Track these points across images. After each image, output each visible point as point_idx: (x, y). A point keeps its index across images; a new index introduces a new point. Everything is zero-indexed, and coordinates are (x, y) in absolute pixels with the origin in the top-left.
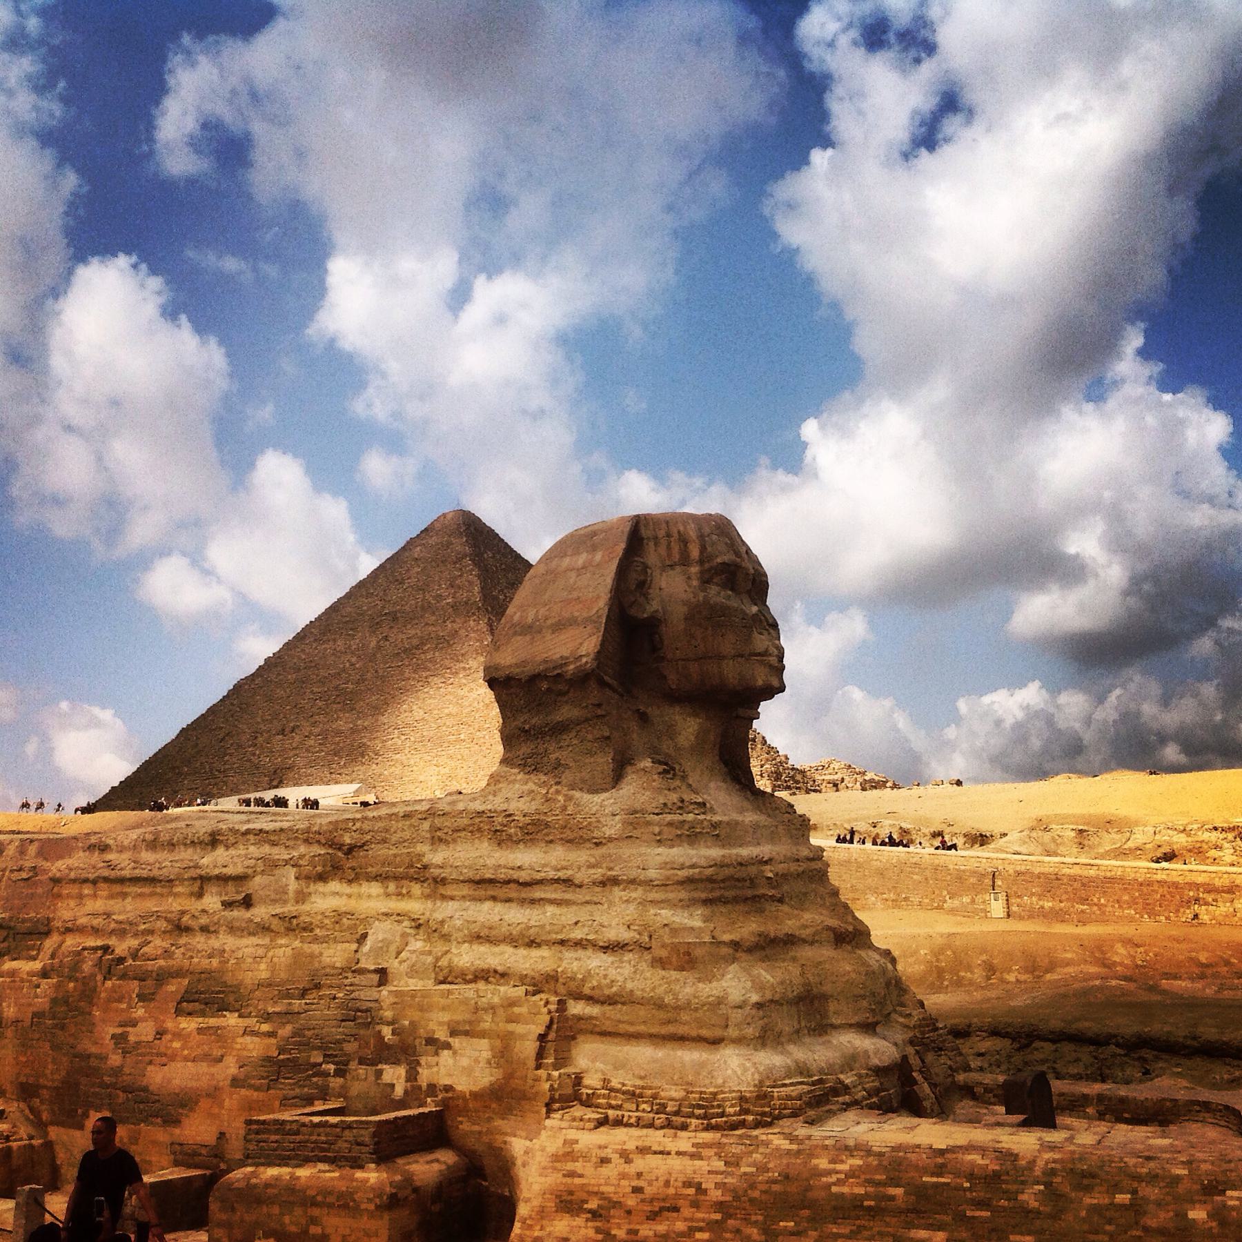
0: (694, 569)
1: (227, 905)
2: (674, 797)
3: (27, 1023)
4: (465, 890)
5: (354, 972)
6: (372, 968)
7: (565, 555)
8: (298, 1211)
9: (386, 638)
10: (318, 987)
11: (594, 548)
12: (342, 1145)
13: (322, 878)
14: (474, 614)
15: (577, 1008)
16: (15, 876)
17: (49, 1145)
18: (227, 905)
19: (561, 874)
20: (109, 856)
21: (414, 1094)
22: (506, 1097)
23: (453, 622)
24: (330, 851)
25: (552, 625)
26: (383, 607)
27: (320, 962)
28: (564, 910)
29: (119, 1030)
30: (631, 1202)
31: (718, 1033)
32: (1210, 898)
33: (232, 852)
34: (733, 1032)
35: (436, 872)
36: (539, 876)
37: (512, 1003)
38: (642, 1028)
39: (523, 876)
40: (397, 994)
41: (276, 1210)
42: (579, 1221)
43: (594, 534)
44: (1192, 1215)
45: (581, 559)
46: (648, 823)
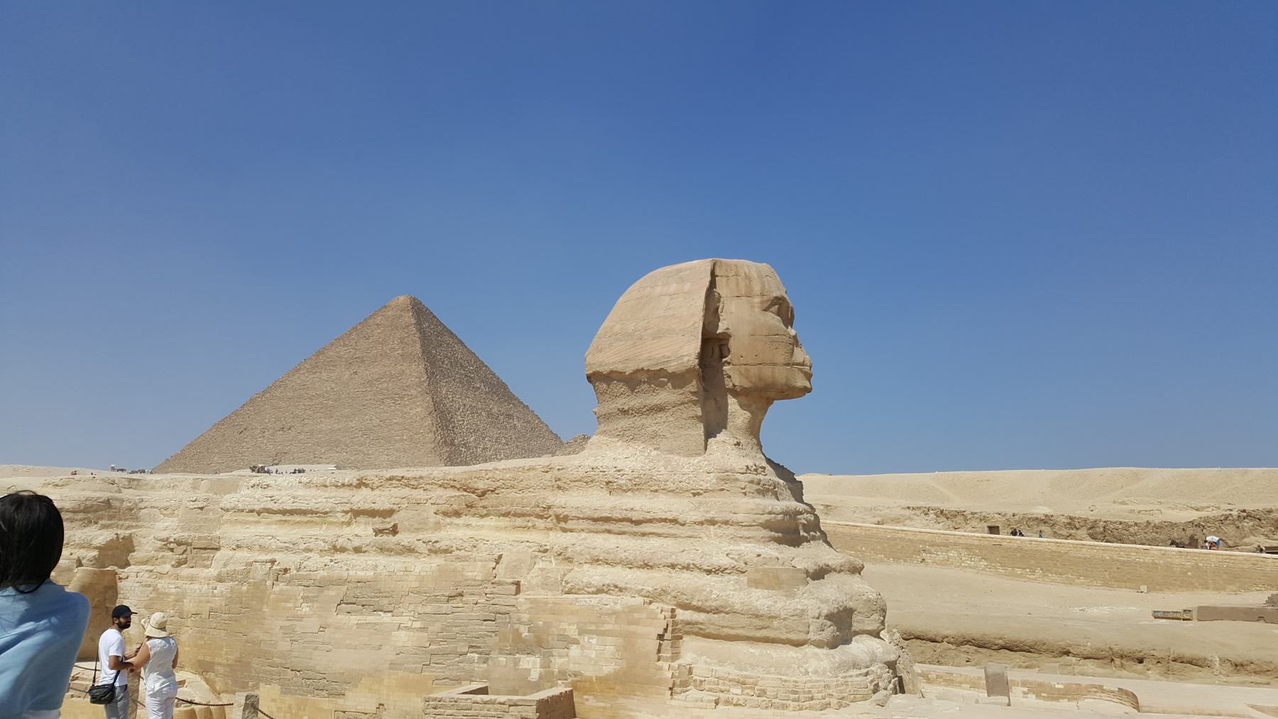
0: (757, 300)
1: (378, 532)
3: (205, 615)
13: (457, 514)
15: (682, 615)
16: (191, 505)
18: (378, 532)
20: (269, 492)
21: (548, 677)
28: (669, 541)
29: (288, 623)
31: (802, 637)
33: (377, 492)
35: (560, 511)
36: (648, 516)
37: (632, 610)
38: (741, 632)
39: (635, 516)
45: (673, 288)
46: (737, 480)
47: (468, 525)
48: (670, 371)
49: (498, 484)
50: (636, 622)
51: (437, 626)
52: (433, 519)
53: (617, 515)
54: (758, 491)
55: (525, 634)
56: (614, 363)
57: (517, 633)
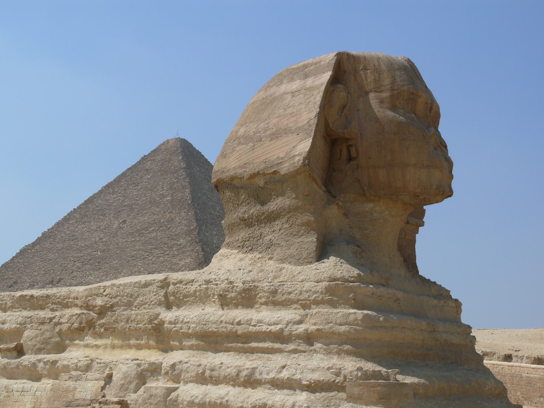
0: (385, 95)
4: (194, 342)
5: (100, 403)
6: (116, 400)
7: (281, 83)
9: (124, 222)
11: (306, 76)
14: (185, 208)
19: (274, 328)
23: (171, 212)
24: (85, 312)
25: (270, 135)
26: (123, 201)
27: (74, 395)
39: (240, 330)
43: (306, 66)
47: (87, 346)
48: (283, 172)
49: (114, 301)
56: (235, 168)
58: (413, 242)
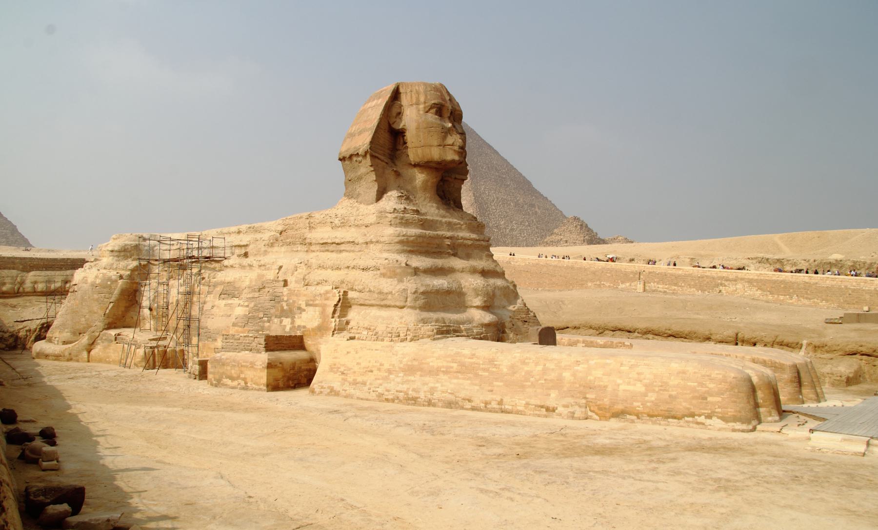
0: (422, 106)
1: (239, 256)
2: (402, 206)
4: (318, 247)
8: (237, 369)
10: (264, 288)
12: (254, 344)
13: (272, 245)
15: (351, 295)
17: (183, 351)
22: (321, 329)
28: (351, 254)
30: (356, 369)
31: (402, 304)
32: (726, 283)
34: (408, 304)
35: (308, 241)
37: (327, 292)
38: (373, 302)
39: (337, 241)
40: (290, 290)
41: (229, 368)
42: (337, 375)
44: (564, 374)
50: (327, 299)
51: (252, 305)
52: (263, 249)
53: (329, 241)
54: (401, 223)
55: (285, 308)
57: (282, 307)
58: (460, 189)
